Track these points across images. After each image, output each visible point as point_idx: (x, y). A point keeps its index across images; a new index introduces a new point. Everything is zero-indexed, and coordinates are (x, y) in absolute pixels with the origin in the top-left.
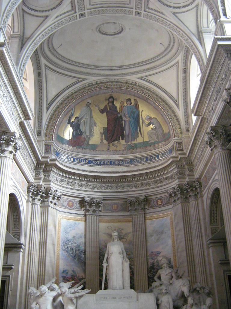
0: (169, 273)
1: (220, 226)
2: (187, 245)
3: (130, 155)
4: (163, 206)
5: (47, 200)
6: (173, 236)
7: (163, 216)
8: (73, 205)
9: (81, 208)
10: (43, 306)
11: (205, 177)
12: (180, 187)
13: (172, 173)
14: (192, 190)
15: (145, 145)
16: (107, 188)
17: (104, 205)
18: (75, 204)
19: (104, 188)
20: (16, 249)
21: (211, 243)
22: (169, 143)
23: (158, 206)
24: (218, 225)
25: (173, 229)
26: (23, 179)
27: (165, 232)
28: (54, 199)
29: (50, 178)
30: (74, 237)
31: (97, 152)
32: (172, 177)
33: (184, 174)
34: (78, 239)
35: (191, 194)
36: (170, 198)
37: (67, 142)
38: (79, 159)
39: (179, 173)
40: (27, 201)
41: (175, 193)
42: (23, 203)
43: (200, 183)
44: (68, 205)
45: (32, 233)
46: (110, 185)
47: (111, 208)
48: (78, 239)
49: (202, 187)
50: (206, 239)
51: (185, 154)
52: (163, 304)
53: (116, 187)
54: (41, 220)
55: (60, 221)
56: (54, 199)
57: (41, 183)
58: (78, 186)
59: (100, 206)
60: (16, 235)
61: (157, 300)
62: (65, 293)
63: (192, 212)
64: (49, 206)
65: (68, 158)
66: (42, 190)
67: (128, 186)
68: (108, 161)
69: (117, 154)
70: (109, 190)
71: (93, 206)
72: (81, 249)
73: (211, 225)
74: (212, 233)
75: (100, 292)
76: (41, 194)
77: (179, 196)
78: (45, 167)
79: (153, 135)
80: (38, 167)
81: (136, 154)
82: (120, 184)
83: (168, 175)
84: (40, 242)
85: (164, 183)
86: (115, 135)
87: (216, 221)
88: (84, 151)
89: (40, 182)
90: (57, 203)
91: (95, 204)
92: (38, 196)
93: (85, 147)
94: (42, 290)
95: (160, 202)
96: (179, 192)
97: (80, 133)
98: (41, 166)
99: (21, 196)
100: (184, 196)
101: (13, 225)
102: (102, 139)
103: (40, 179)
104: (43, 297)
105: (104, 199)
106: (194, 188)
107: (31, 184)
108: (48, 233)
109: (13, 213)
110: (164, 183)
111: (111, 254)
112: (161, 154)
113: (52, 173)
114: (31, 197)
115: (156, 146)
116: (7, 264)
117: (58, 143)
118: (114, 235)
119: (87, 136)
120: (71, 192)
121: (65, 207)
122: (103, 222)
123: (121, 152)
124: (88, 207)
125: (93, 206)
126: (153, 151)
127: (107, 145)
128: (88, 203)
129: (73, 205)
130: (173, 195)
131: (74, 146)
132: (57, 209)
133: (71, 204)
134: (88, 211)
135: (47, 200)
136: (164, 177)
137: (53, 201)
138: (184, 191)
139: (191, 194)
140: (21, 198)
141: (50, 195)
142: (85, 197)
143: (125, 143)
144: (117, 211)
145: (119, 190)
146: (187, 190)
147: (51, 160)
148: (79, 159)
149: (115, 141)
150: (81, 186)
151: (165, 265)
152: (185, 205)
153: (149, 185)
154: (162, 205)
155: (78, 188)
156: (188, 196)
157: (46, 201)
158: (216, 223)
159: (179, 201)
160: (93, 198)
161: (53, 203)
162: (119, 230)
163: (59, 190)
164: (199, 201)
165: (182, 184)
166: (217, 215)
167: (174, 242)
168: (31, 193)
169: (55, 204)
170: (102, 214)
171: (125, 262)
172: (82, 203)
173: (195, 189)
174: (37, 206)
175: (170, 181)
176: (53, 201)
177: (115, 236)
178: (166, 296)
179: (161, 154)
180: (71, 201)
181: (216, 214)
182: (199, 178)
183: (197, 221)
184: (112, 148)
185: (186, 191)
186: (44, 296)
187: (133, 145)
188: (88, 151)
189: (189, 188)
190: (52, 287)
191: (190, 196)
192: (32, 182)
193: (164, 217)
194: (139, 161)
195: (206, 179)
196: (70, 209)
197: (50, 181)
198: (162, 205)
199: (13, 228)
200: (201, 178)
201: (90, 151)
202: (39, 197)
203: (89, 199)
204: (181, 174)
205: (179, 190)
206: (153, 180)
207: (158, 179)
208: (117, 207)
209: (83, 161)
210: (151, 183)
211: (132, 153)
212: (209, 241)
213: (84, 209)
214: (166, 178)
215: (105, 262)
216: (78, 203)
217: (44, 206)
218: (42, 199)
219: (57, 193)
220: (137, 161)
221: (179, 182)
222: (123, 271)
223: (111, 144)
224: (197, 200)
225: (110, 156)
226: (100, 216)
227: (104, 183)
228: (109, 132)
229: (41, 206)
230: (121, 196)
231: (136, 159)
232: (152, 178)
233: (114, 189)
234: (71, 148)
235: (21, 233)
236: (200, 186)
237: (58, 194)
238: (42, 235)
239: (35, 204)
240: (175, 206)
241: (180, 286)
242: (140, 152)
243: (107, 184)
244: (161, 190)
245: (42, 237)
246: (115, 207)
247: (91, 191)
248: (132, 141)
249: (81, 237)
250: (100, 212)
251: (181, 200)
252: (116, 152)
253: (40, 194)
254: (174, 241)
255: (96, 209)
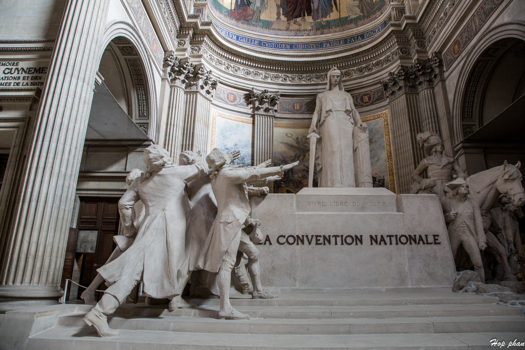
0: (449, 163)
1: (477, 123)
2: (416, 155)
3: (320, 36)
4: (372, 104)
5: (195, 83)
6: (390, 145)
7: (372, 118)
8: (235, 99)
9: (248, 104)
10: (154, 203)
11: (456, 42)
12: (403, 68)
13: (389, 54)
14: (423, 74)
15: (343, 22)
16: (285, 80)
17: (280, 103)
18: (238, 99)
19: (281, 79)
20: (139, 149)
21: (463, 147)
22: (382, 13)
23: (364, 104)
24: (473, 121)
25: (389, 135)
26: (154, 37)
27: (376, 141)
28: (206, 84)
29: (201, 53)
30: (236, 145)
31: (271, 31)
32: (387, 60)
33: (409, 53)
34: (242, 148)
35: (421, 79)
36: (385, 89)
37: (228, 12)
38: (245, 38)
39: (401, 50)
40: (163, 79)
41: (394, 80)
42: (153, 74)
43: (441, 61)
44: (228, 98)
45: (170, 128)
46: (290, 75)
47: (292, 108)
48: (242, 148)
49: (443, 65)
50: (452, 144)
51: (414, 18)
52: (459, 221)
53: (300, 78)
54: (186, 112)
55: (214, 119)
56: (206, 84)
57: (187, 56)
58: (243, 73)
59: (276, 104)
60: (142, 127)
61: (445, 211)
62: (221, 166)
63: (424, 106)
64: (198, 92)
65: (229, 35)
66: (187, 65)
67: (317, 78)
68: (288, 44)
69: (300, 34)
70: (289, 83)
71: (265, 102)
72: (246, 163)
73: (463, 121)
74: (465, 134)
75: (304, 191)
76: (186, 72)
77: (402, 83)
78: (193, 35)
79: (355, 8)
80: (182, 33)
81: (329, 35)
82: (305, 75)
83: (380, 59)
84: (182, 145)
85: (373, 71)
86: (298, 9)
87: (472, 115)
88: (252, 28)
89: (185, 55)
90: (210, 91)
91: (268, 99)
92: (180, 75)
93: (253, 23)
94: (151, 156)
95: (366, 98)
96: (403, 78)
97: (247, 2)
98: (187, 32)
99: (149, 59)
100: (409, 83)
101: (137, 110)
102: (278, 14)
103: (185, 50)
104: (156, 178)
105: (282, 95)
106: (428, 69)
107: (170, 54)
108: (195, 131)
109: (137, 90)
110: (373, 71)
111: (327, 112)
112: (368, 33)
113: (203, 47)
114: (170, 75)
115: (360, 22)
116: (125, 170)
117: (214, 8)
118: (334, 76)
119: (258, 8)
120: (233, 80)
121: (223, 100)
122: (280, 127)
123: (307, 32)
124: (257, 104)
125: (265, 102)
126: (354, 29)
127: (286, 23)
128: (257, 97)
129: (235, 99)
130: (391, 84)
131: (238, 20)
132: (211, 101)
133: (232, 97)
134: (258, 109)
135: (195, 83)
136: (374, 62)
137: (204, 86)
138: (411, 75)
139: (421, 79)
140: (150, 63)
141: (200, 76)
142: (253, 88)
143: (312, 21)
144: (301, 111)
145: (304, 83)
146: (415, 74)
147: (203, 24)
148: (245, 38)
149: (297, 17)
150: (248, 73)
151: (439, 148)
152: (411, 96)
153: (348, 76)
154: (370, 103)
155: (244, 76)
156: (417, 83)
157: (194, 85)
158: (472, 117)
159: (401, 92)
160: (265, 92)
161: (205, 90)
162: (303, 139)
163: (213, 73)
164: (438, 89)
165: (407, 67)
166: (475, 104)
167: (391, 155)
168: (169, 69)
169: (208, 92)
170: (277, 115)
171: (360, 130)
172: (249, 97)
173: (429, 70)
174: (179, 90)
175: (384, 66)
176: (204, 86)
177: (336, 78)
178: (466, 203)
179: (368, 33)
180: (232, 94)
181: (473, 102)
182: (438, 52)
183: (433, 119)
184: (294, 27)
185: (413, 76)
186: (160, 175)
187: (324, 24)
188: (258, 29)
189: (419, 71)
190: (185, 159)
191: (420, 83)
192: (172, 51)
193: (373, 119)
194: (333, 44)
195: (459, 45)
196: (231, 105)
197: (200, 56)
198: (370, 103)
199: (137, 115)
200: (441, 53)
201: (261, 29)
202: (182, 77)
203: (260, 92)
204: (405, 53)
205: (403, 74)
206: (355, 68)
207: (364, 65)
208: (301, 107)
209: (251, 42)
210: (353, 72)
211: (322, 33)
212: (461, 145)
213: (251, 106)
214: (378, 64)
215: (314, 131)
216: (242, 97)
217: (191, 93)
218: (187, 81)
219: (212, 76)
220: (330, 44)
221: (401, 63)
222: (355, 150)
223: (292, 22)
224: (433, 88)
225: (291, 37)
226: (274, 117)
227: (281, 71)
228: (289, 5)
229: (186, 93)
230: (307, 91)
231: (328, 42)
232: (354, 65)
233: (297, 82)
234: (234, 22)
235: (149, 124)
236: (441, 66)
237: (214, 78)
238: (187, 134)
239: (176, 86)
240: (394, 100)
241: (494, 183)
242: (335, 32)
243: (287, 75)
244: (369, 80)
245: (186, 137)
246: (297, 107)
247: (262, 82)
248: (322, 17)
249: (246, 146)
250: (275, 113)
251: (406, 90)
252: (298, 32)
253: (184, 73)
254: (390, 153)
255: (270, 108)
